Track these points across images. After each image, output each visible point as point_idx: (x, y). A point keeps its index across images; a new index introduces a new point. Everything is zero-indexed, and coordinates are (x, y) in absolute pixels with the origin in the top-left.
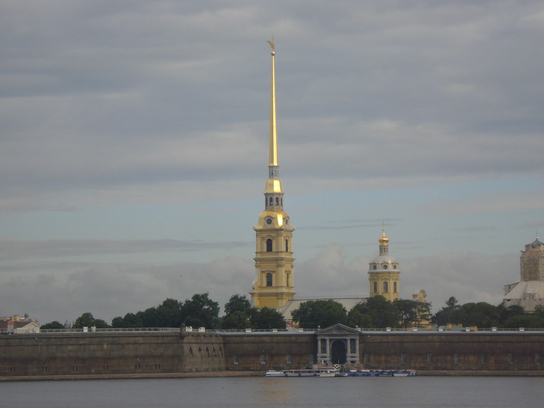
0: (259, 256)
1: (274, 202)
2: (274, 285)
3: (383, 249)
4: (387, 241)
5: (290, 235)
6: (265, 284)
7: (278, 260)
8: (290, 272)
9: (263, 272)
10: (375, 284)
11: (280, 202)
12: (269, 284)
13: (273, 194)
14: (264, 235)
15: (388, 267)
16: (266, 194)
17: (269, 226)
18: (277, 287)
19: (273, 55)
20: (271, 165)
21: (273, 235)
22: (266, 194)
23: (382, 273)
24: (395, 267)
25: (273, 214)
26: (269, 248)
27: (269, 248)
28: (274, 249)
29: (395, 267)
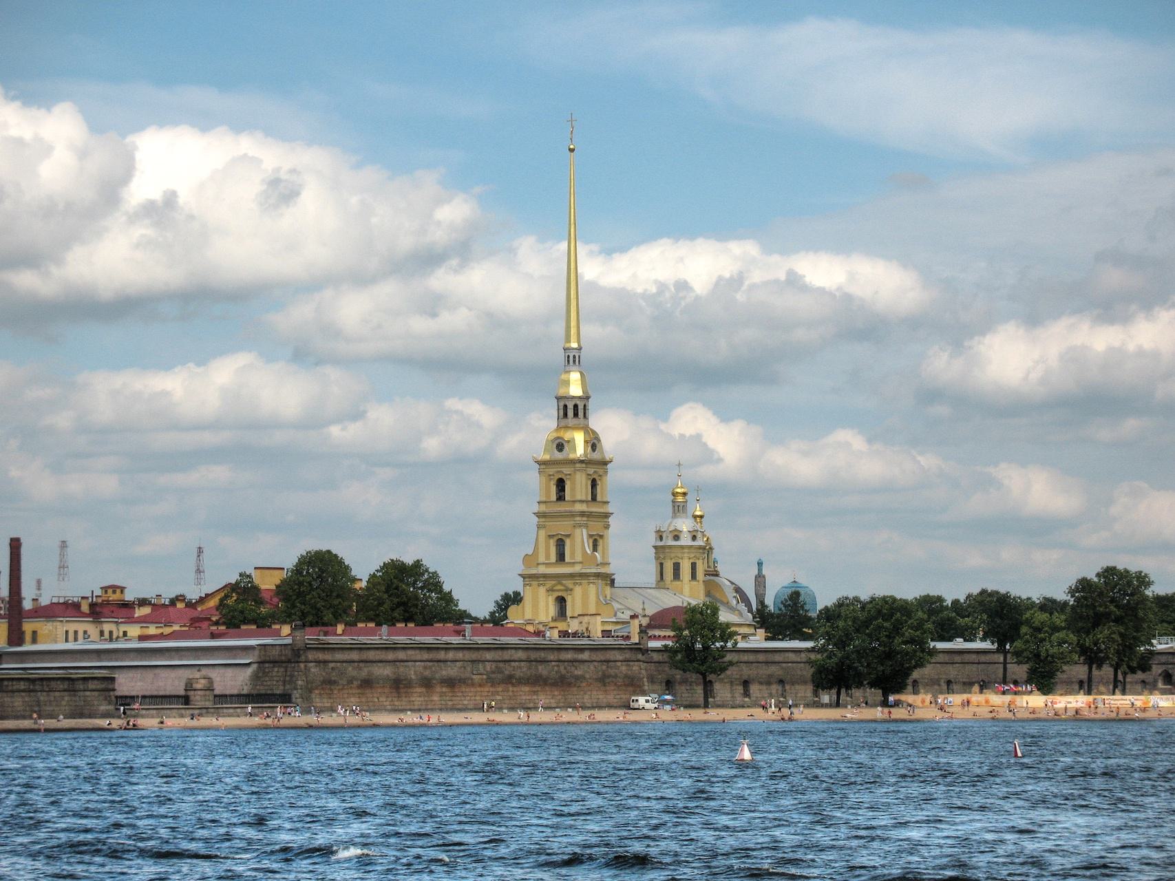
0: (543, 508)
1: (570, 413)
2: (567, 559)
4: (685, 494)
5: (601, 472)
7: (573, 516)
8: (601, 537)
9: (551, 537)
10: (662, 564)
15: (682, 537)
17: (596, 456)
19: (572, 150)
20: (567, 345)
21: (601, 472)
23: (670, 547)
24: (694, 538)
25: (567, 436)
28: (599, 498)
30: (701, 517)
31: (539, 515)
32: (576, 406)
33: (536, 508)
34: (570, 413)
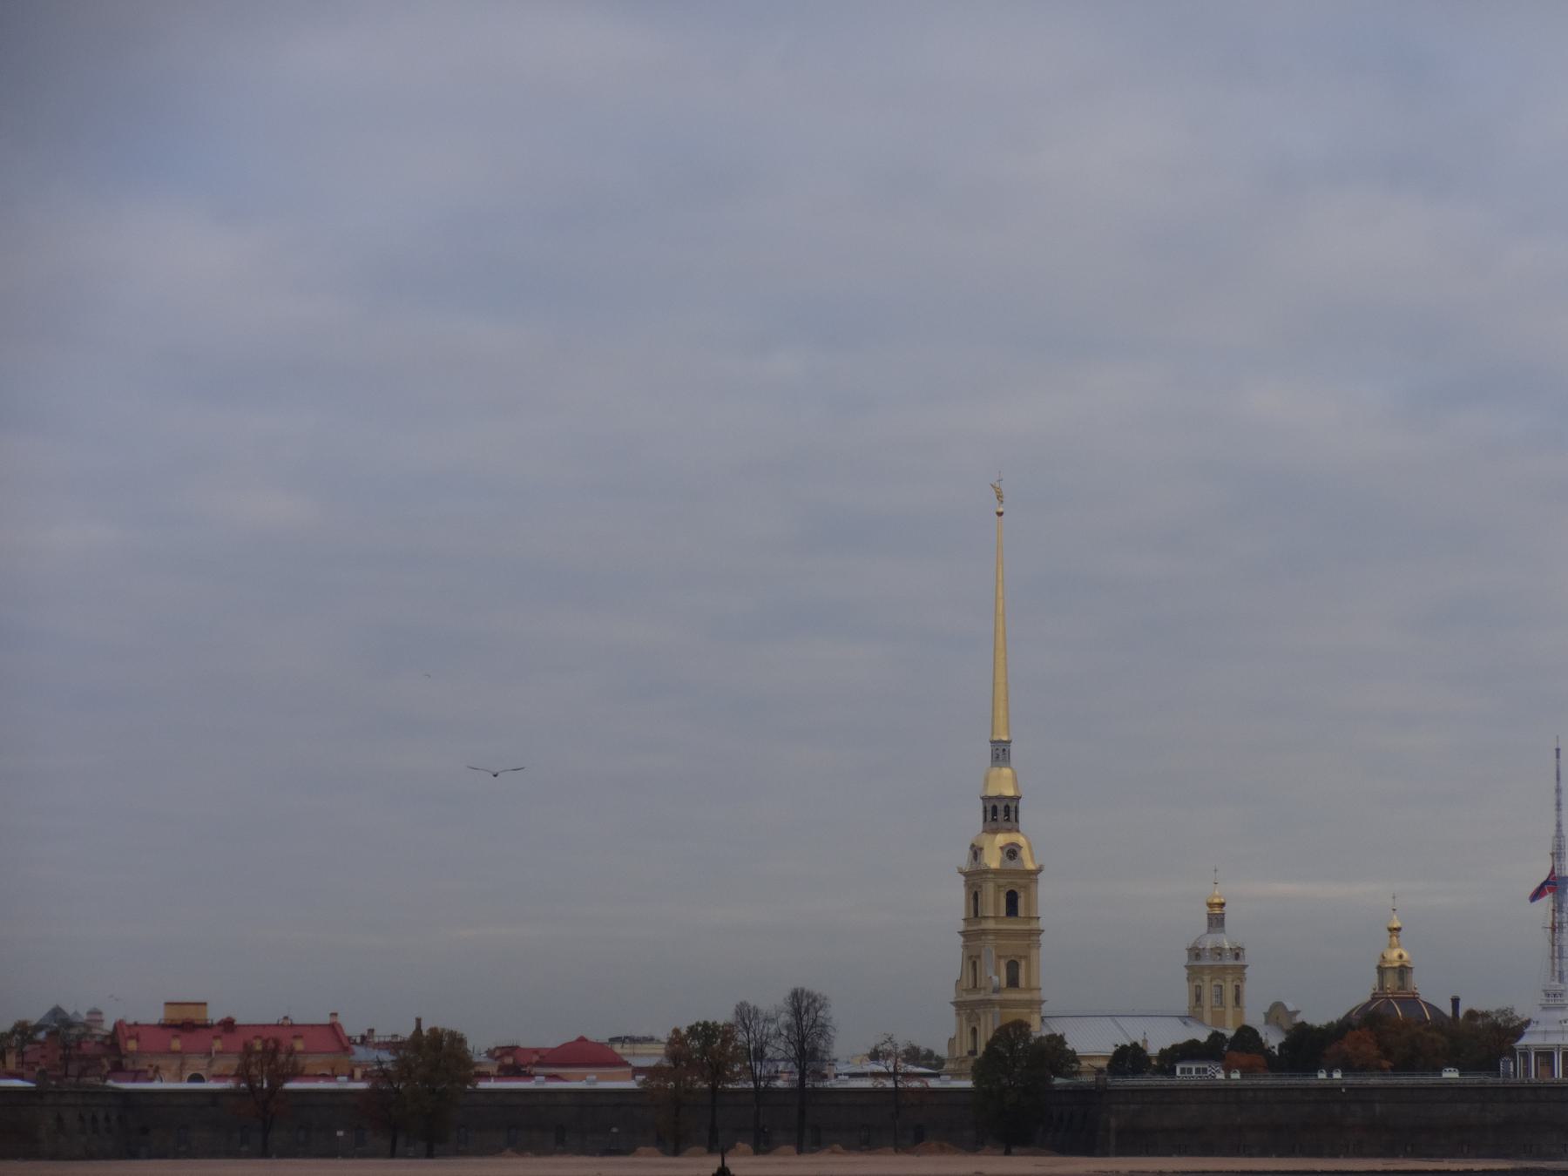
3: (1216, 920)
4: (1222, 905)
6: (1004, 983)
11: (1012, 815)
12: (1013, 982)
13: (1000, 798)
14: (1002, 881)
16: (985, 799)
17: (1012, 865)
18: (1029, 989)
19: (1000, 514)
20: (996, 738)
22: (985, 799)
26: (1012, 908)
27: (1012, 908)
28: (1021, 913)
29: (1237, 956)
30: (1398, 929)
31: (964, 934)
32: (995, 808)
33: (961, 926)
34: (989, 817)
